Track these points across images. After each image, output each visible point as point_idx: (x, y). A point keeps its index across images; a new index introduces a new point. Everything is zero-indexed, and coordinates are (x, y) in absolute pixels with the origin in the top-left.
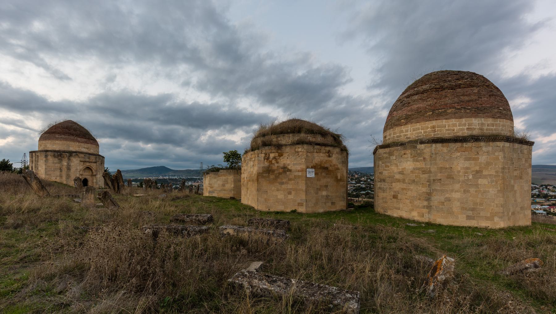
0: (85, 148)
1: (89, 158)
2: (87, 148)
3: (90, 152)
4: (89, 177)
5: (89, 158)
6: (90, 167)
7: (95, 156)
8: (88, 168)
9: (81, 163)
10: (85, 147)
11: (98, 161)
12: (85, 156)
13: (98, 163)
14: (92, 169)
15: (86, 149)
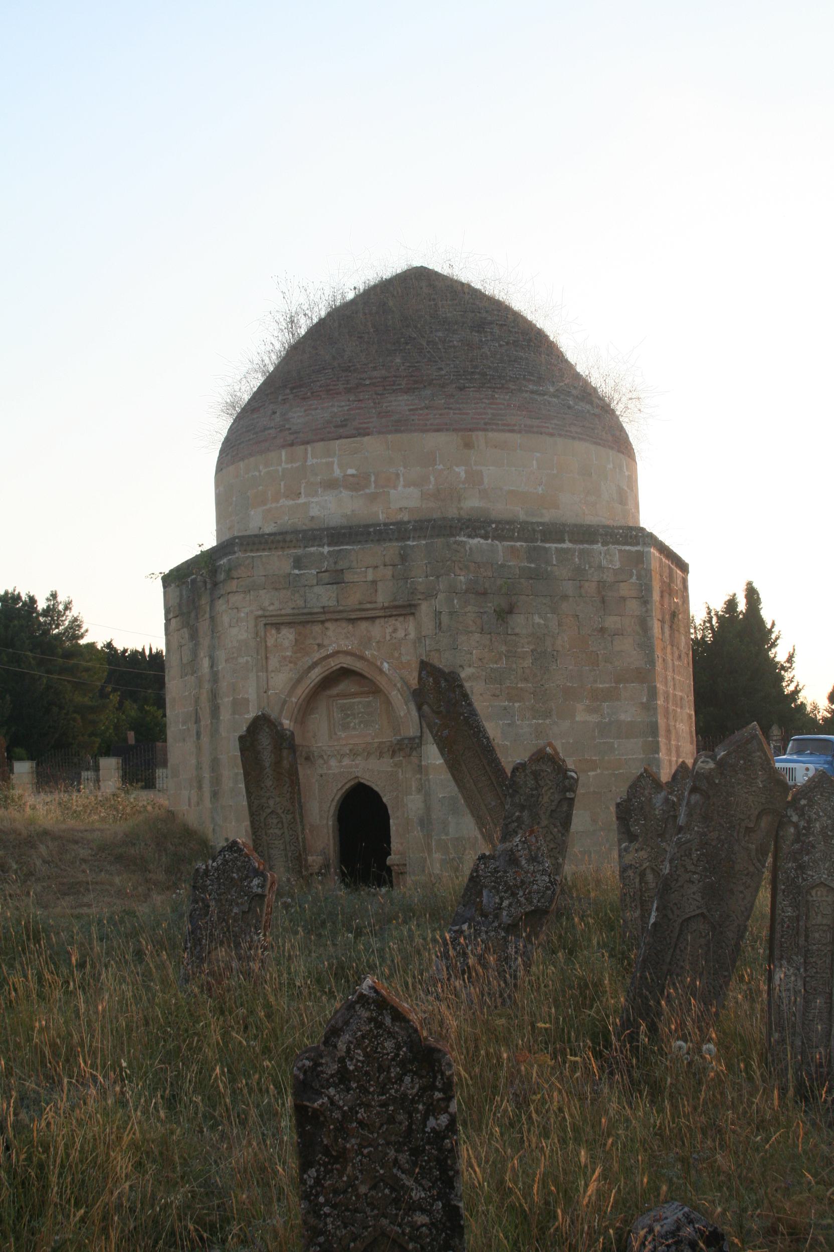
0: (331, 485)
1: (337, 578)
2: (356, 484)
3: (380, 514)
4: (385, 765)
5: (337, 578)
6: (357, 665)
7: (391, 549)
8: (345, 673)
9: (272, 637)
10: (337, 472)
11: (430, 595)
12: (298, 563)
13: (425, 608)
14: (382, 682)
15: (345, 494)
